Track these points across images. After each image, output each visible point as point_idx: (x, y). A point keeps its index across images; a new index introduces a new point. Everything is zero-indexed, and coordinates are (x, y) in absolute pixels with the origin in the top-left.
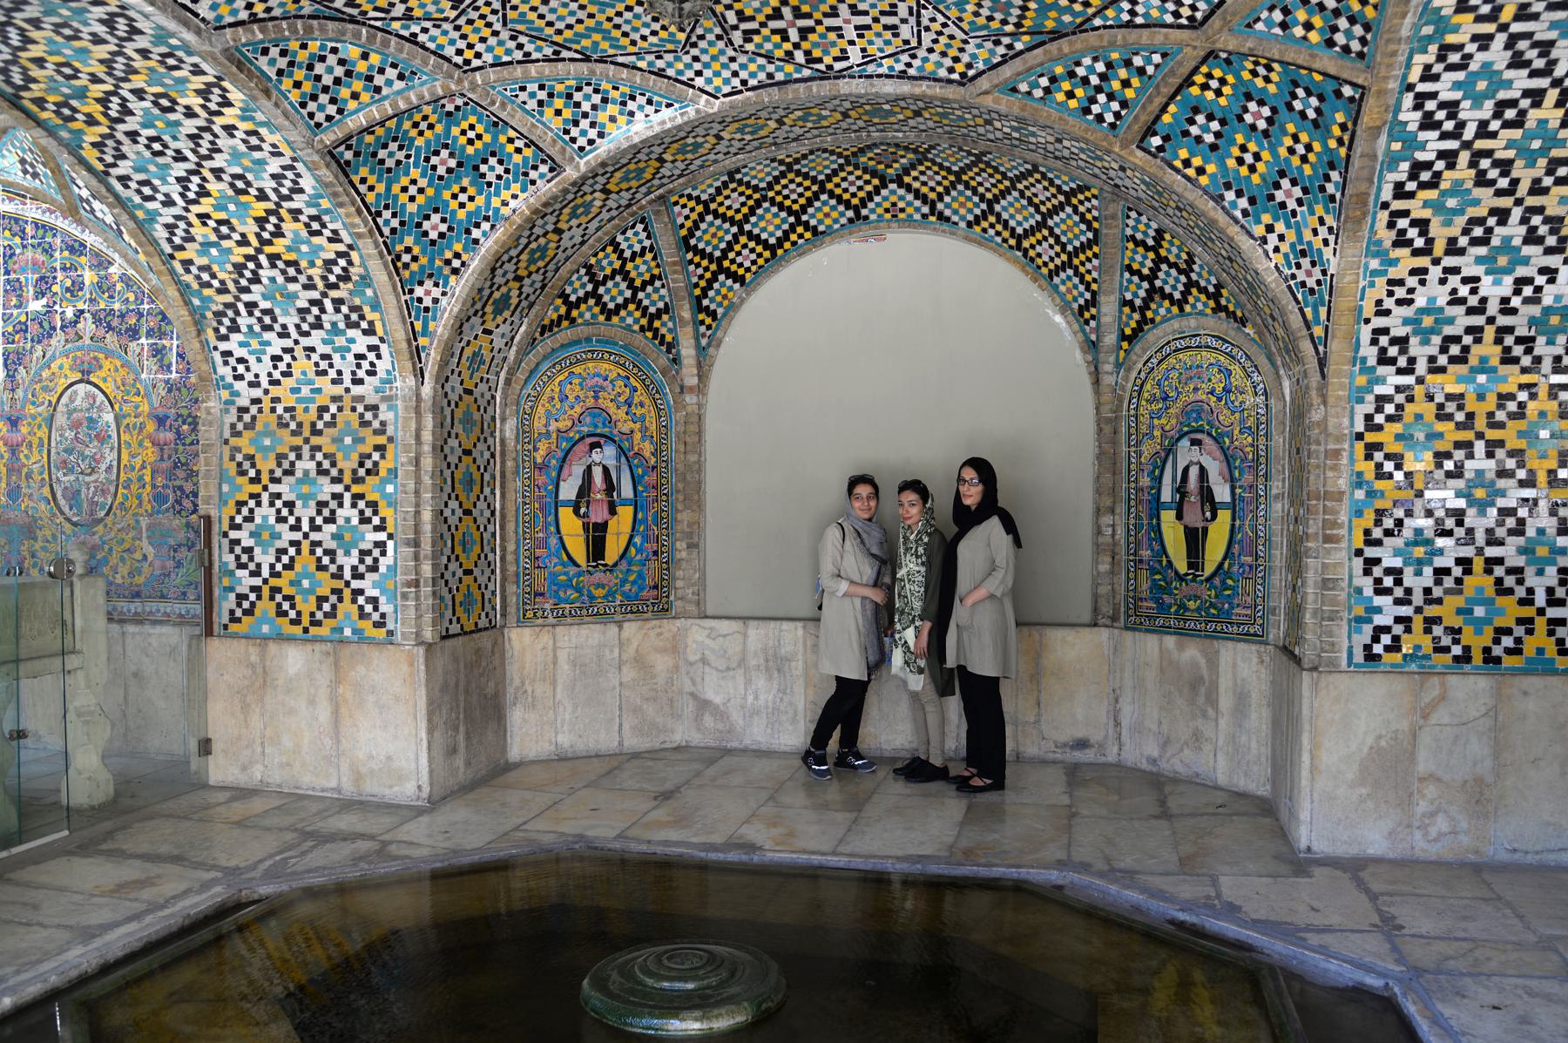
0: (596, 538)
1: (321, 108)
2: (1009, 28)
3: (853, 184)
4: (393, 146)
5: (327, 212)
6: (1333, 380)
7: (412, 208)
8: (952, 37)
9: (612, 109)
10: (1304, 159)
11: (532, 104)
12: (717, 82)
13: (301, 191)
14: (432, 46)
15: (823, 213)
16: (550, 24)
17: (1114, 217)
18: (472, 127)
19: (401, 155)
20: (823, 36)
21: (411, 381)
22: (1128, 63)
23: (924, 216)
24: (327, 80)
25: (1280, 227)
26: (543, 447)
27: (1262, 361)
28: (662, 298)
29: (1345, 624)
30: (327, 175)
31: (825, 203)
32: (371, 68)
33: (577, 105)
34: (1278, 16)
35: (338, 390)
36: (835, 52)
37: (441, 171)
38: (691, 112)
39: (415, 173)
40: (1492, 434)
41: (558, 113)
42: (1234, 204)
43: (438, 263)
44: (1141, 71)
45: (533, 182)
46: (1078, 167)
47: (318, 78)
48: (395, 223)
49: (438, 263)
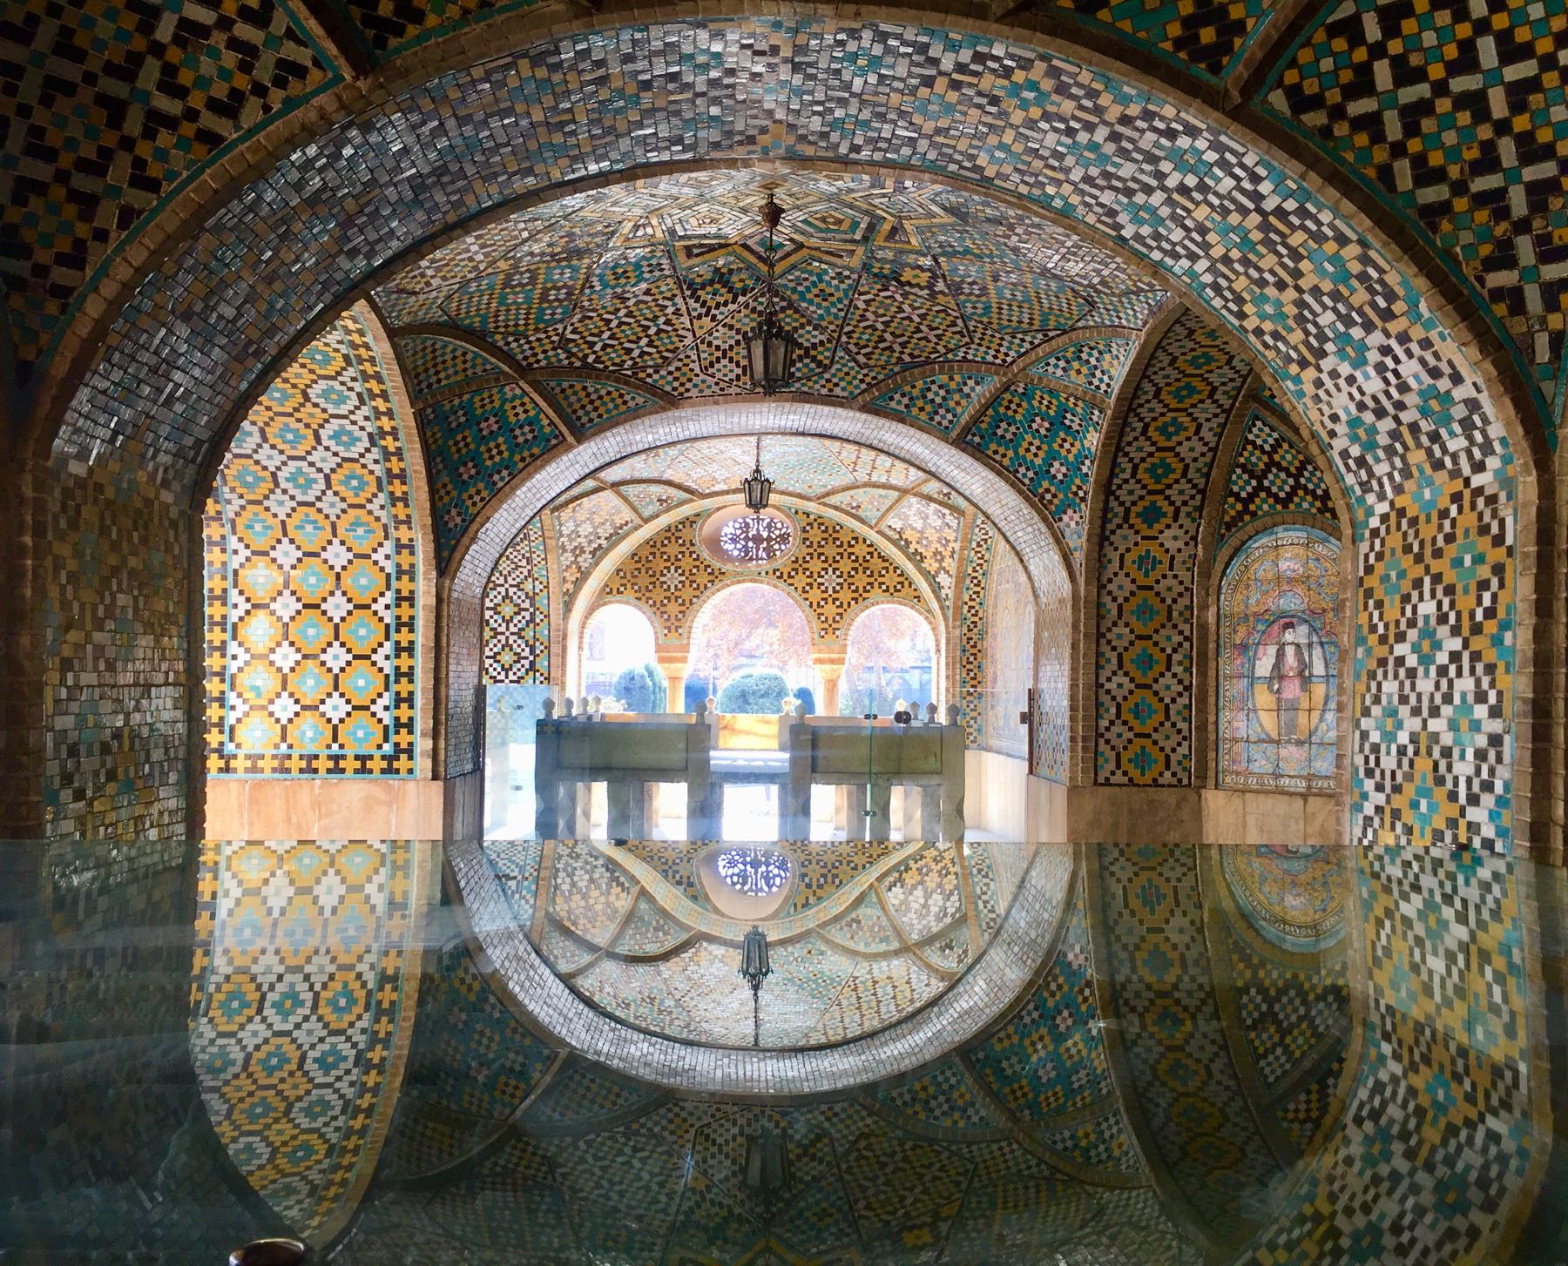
1: (944, 417)
7: (1038, 461)
9: (1107, 357)
11: (1059, 372)
19: (1012, 429)
29: (1347, 809)
33: (1088, 362)
37: (1043, 431)
41: (1079, 372)
47: (932, 401)
48: (1031, 474)
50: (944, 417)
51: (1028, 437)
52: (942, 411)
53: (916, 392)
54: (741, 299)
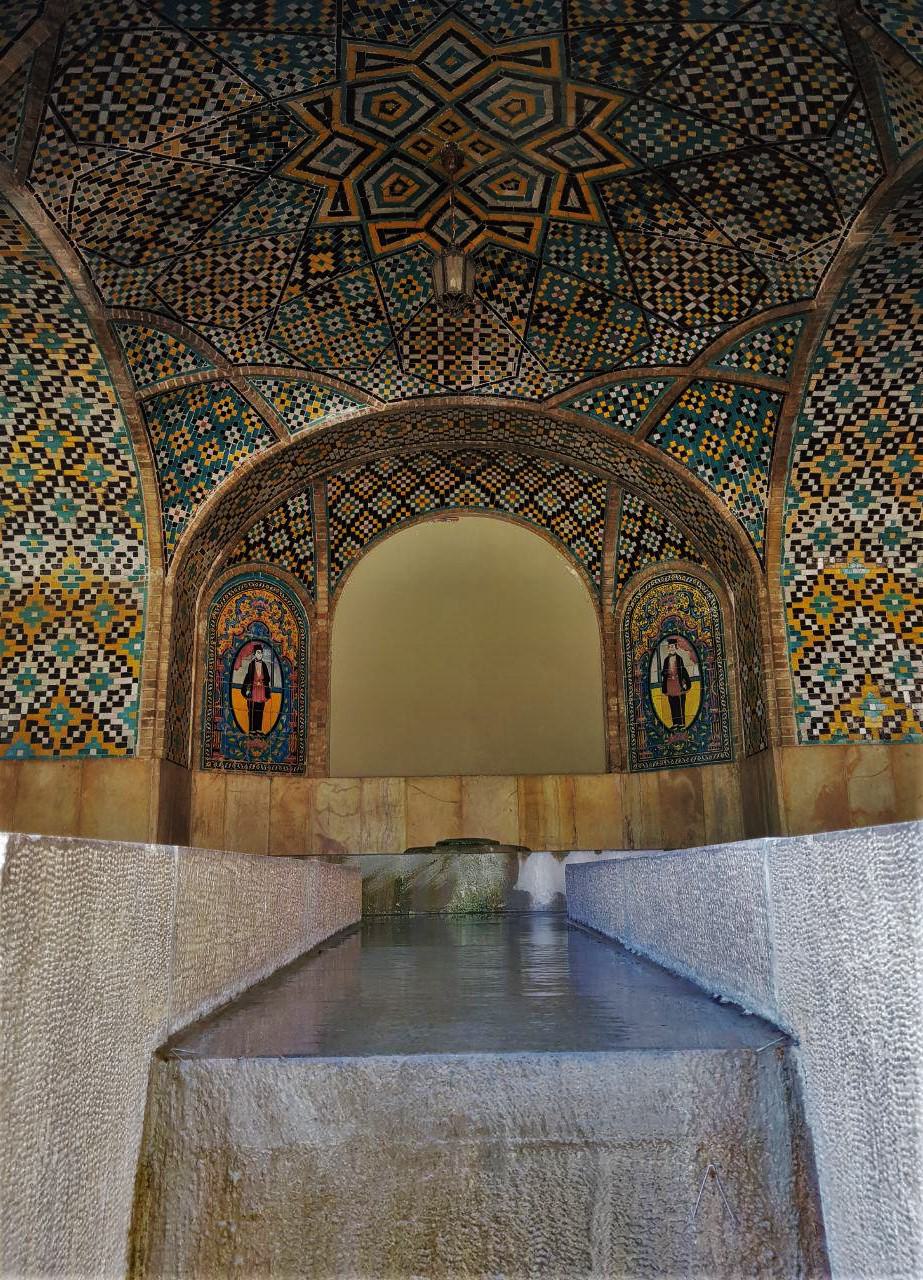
0: (256, 712)
2: (573, 367)
3: (443, 479)
4: (177, 408)
5: (124, 447)
6: (770, 572)
7: (178, 453)
8: (537, 372)
9: (316, 404)
10: (747, 442)
12: (387, 392)
13: (111, 430)
14: (218, 345)
15: (422, 499)
16: (294, 342)
17: (616, 498)
18: (227, 404)
20: (459, 367)
21: (160, 572)
22: (643, 389)
23: (486, 504)
24: (152, 356)
25: (732, 485)
26: (223, 644)
27: (714, 584)
28: (309, 549)
30: (136, 418)
31: (422, 492)
32: (178, 353)
33: (295, 398)
34: (735, 357)
35: (99, 578)
36: (464, 378)
38: (367, 410)
39: (185, 429)
40: (865, 603)
41: (283, 402)
42: (704, 474)
43: (187, 493)
44: (651, 393)
45: (257, 447)
46: (598, 465)
48: (166, 461)
49: (187, 493)
50: (144, 373)
51: (185, 429)
52: (147, 367)
53: (144, 336)
54: (231, 163)
